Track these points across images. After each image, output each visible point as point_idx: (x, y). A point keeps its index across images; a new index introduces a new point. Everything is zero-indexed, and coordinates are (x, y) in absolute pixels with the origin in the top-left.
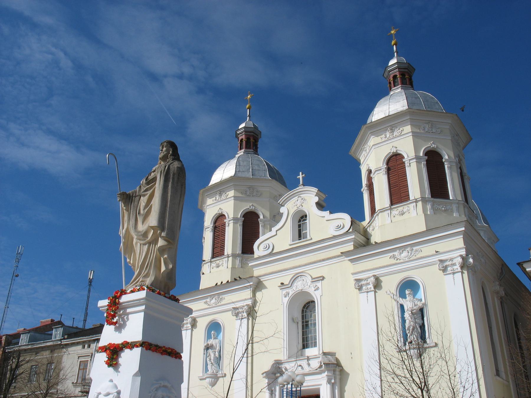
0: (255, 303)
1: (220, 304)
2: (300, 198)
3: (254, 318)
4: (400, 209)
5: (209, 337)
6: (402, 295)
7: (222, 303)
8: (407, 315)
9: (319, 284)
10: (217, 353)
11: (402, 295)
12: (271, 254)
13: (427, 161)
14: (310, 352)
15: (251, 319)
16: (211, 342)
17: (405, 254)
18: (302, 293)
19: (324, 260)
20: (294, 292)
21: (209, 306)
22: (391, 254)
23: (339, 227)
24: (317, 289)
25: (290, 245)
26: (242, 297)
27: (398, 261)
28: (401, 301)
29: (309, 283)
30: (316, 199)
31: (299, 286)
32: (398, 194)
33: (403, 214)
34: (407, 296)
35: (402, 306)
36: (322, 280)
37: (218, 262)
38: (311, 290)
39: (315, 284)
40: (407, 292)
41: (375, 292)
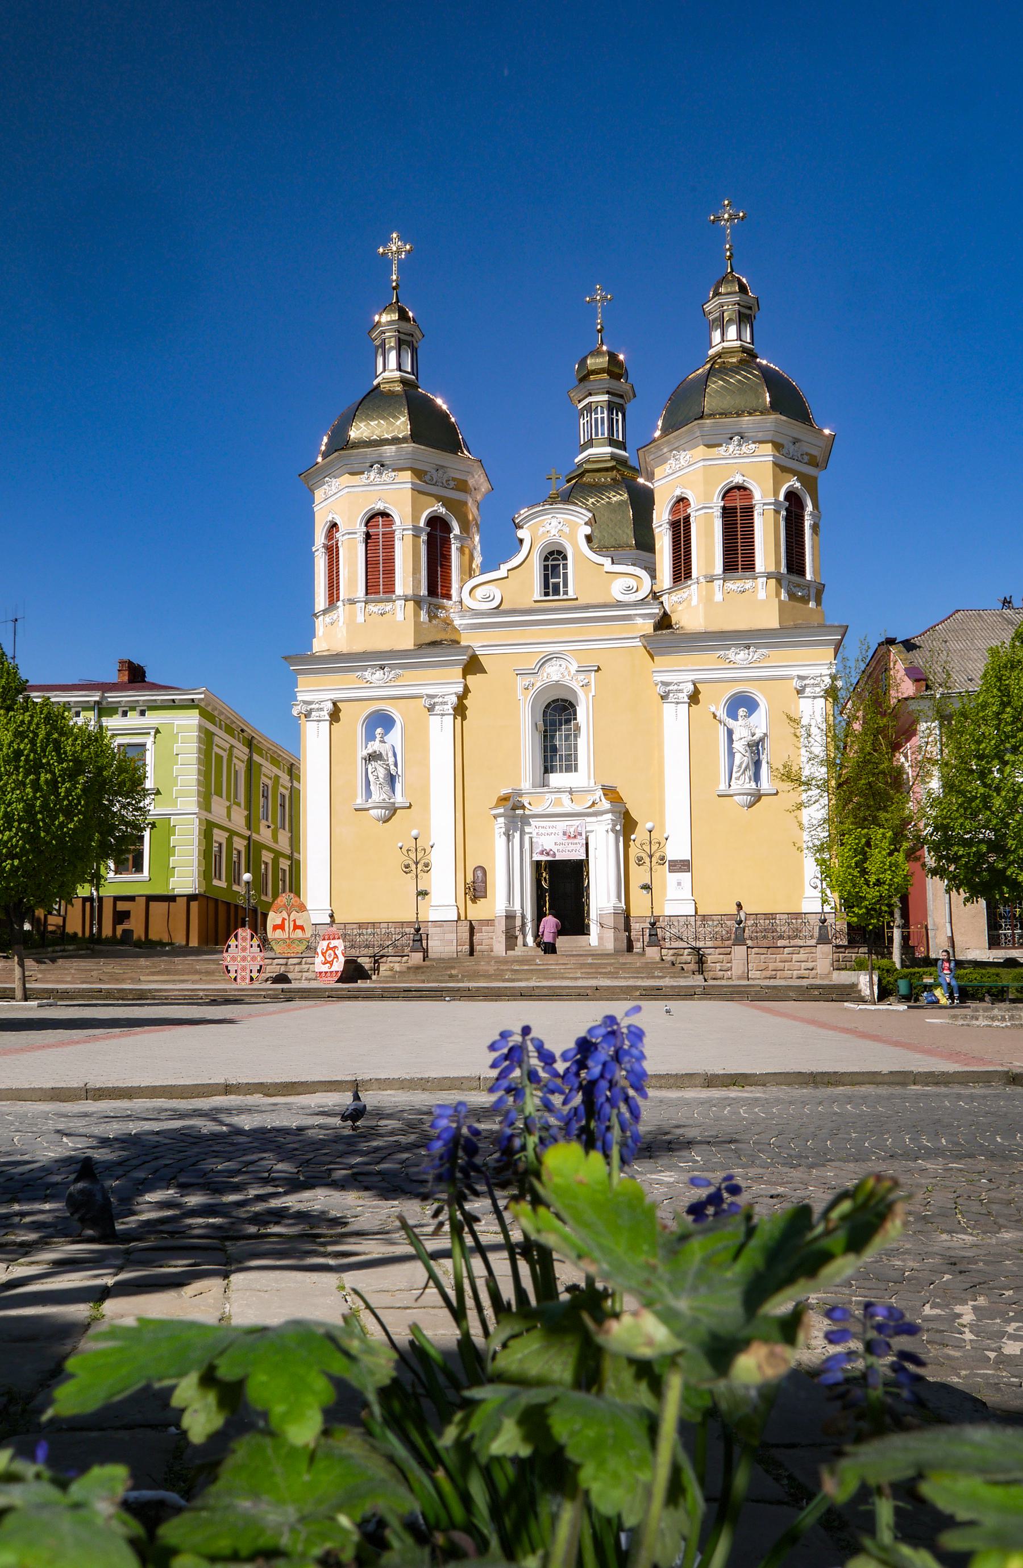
0: (467, 690)
3: (464, 718)
5: (370, 737)
6: (733, 714)
10: (392, 767)
11: (733, 714)
12: (497, 610)
14: (556, 779)
15: (459, 718)
16: (375, 746)
18: (557, 685)
21: (368, 685)
25: (535, 601)
27: (731, 665)
28: (731, 723)
29: (573, 672)
30: (588, 530)
31: (553, 673)
35: (730, 733)
36: (596, 671)
38: (575, 686)
40: (742, 712)
41: (690, 706)
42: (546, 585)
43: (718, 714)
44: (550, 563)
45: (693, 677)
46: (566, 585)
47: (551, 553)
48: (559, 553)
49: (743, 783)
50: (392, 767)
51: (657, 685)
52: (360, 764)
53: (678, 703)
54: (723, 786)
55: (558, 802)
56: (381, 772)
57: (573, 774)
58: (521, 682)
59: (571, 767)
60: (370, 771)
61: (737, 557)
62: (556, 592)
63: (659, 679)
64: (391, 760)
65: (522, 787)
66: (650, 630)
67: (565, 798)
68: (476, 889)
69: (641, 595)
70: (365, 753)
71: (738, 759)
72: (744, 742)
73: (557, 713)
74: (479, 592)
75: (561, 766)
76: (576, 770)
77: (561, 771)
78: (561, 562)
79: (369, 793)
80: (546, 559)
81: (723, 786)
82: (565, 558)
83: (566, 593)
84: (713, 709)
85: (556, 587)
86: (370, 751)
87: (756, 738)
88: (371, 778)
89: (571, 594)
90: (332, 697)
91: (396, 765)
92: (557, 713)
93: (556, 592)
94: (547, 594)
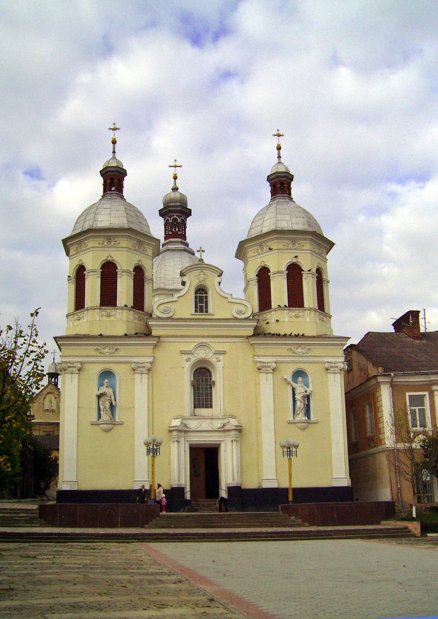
1: (114, 355)
2: (202, 273)
4: (297, 312)
5: (101, 385)
7: (117, 355)
8: (298, 397)
9: (221, 357)
13: (317, 277)
16: (103, 390)
17: (299, 350)
18: (203, 361)
19: (227, 337)
20: (195, 359)
22: (288, 347)
23: (240, 312)
24: (219, 361)
26: (141, 353)
28: (294, 385)
31: (201, 354)
32: (295, 299)
33: (297, 317)
34: (299, 383)
35: (293, 390)
37: (109, 311)
38: (214, 360)
39: (217, 356)
42: (196, 307)
43: (288, 380)
44: (198, 295)
45: (275, 360)
46: (206, 307)
48: (203, 290)
49: (301, 417)
50: (113, 402)
51: (257, 363)
52: (95, 399)
53: (267, 373)
54: (291, 419)
56: (108, 404)
57: (210, 409)
58: (186, 357)
59: (208, 404)
60: (100, 403)
63: (259, 360)
64: (113, 398)
65: (185, 415)
66: (251, 333)
69: (248, 314)
70: (99, 393)
71: (298, 403)
72: (302, 395)
74: (162, 307)
75: (203, 405)
76: (211, 407)
77: (203, 407)
78: (204, 295)
79: (100, 416)
80: (196, 293)
81: (291, 419)
82: (206, 293)
83: (207, 311)
85: (201, 307)
86: (102, 392)
87: (308, 393)
88: (102, 407)
90: (81, 360)
91: (115, 401)
93: (201, 311)
94: (196, 311)
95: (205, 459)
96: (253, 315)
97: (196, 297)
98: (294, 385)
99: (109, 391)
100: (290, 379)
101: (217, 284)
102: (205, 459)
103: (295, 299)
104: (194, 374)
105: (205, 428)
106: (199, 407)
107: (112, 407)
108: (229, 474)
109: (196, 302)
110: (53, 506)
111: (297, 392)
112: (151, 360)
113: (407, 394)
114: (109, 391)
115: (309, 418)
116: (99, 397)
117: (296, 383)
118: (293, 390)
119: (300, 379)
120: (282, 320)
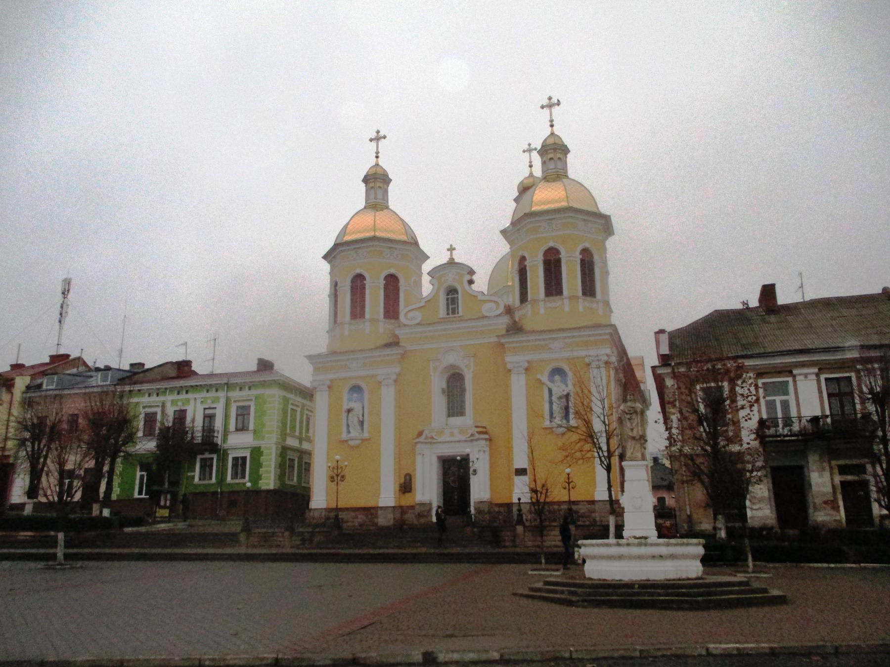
5: (350, 400)
8: (554, 398)
16: (352, 405)
18: (452, 366)
35: (550, 391)
38: (462, 366)
47: (451, 291)
49: (558, 421)
52: (344, 415)
55: (452, 434)
56: (356, 420)
61: (553, 286)
62: (454, 312)
64: (361, 413)
66: (504, 332)
67: (456, 431)
68: (406, 487)
71: (555, 407)
73: (455, 383)
74: (411, 315)
79: (349, 432)
80: (448, 295)
84: (539, 376)
87: (565, 393)
88: (350, 423)
89: (460, 314)
92: (455, 383)
94: (448, 314)
95: (456, 473)
96: (509, 311)
97: (447, 299)
98: (550, 385)
99: (356, 406)
100: (545, 379)
101: (466, 284)
102: (456, 473)
103: (553, 286)
104: (448, 381)
105: (454, 437)
106: (453, 416)
107: (362, 423)
108: (480, 491)
109: (448, 305)
110: (127, 526)
111: (553, 393)
112: (397, 370)
113: (698, 387)
114: (356, 406)
115: (568, 421)
116: (349, 411)
117: (552, 381)
118: (550, 391)
119: (557, 378)
120: (540, 311)
